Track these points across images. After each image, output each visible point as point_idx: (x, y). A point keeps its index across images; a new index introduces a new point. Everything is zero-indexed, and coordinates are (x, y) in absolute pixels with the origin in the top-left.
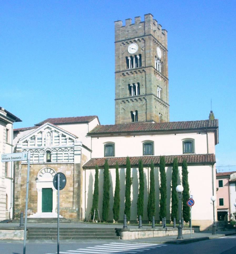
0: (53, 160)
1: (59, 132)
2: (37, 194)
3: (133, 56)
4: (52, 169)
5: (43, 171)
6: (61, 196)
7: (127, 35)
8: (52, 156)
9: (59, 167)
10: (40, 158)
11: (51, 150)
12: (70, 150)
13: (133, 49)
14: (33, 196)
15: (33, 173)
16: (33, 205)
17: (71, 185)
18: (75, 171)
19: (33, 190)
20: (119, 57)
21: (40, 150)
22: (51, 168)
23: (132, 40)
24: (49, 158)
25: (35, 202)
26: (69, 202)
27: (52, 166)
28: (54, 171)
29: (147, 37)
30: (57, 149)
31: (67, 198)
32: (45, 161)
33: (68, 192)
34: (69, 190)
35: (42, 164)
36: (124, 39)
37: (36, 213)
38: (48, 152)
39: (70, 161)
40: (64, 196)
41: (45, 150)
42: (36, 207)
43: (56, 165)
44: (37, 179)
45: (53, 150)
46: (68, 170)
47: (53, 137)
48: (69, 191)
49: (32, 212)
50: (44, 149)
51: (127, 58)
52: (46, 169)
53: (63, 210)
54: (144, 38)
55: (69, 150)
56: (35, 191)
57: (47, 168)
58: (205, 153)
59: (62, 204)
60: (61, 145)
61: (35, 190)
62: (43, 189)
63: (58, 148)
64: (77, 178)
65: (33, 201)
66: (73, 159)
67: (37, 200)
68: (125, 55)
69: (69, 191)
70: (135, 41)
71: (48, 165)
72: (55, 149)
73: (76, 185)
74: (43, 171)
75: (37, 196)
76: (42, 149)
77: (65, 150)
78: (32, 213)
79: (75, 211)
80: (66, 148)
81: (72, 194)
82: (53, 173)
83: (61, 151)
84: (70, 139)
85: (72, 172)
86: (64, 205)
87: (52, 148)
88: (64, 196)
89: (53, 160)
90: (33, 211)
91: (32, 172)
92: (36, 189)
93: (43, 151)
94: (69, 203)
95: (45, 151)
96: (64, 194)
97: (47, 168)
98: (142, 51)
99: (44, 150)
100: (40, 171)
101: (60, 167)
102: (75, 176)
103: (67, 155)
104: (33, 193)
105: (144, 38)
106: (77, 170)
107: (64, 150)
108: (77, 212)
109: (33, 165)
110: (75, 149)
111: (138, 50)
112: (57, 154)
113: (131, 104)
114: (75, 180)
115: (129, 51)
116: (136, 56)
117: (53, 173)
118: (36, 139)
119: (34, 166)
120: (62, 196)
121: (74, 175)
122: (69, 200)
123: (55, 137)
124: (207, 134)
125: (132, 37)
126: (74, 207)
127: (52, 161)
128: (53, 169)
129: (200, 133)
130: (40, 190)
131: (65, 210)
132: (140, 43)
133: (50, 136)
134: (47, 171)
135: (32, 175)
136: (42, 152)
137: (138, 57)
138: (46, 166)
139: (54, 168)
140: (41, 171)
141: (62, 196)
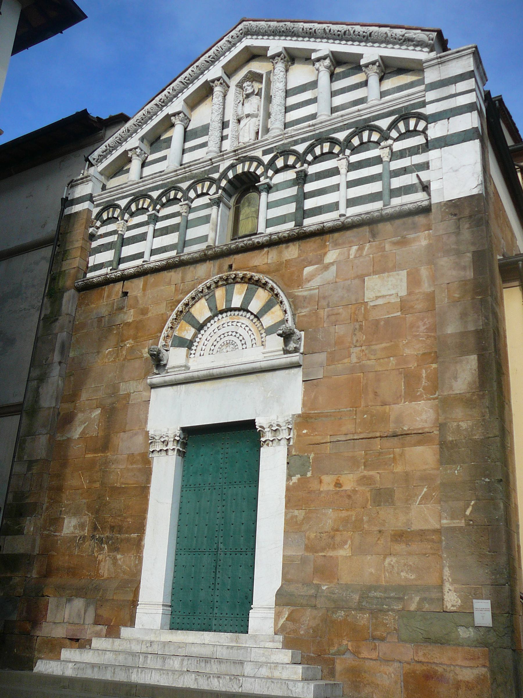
2: (147, 472)
4: (258, 283)
6: (328, 482)
9: (310, 264)
11: (260, 163)
12: (394, 134)
14: (116, 491)
16: (115, 559)
19: (126, 444)
21: (192, 186)
22: (249, 274)
25: (128, 540)
26: (400, 536)
27: (259, 259)
28: (278, 290)
30: (301, 148)
31: (382, 497)
33: (388, 443)
34: (392, 427)
37: (125, 632)
40: (349, 481)
41: (224, 175)
42: (132, 584)
44: (158, 362)
46: (382, 267)
48: (395, 436)
49: (96, 623)
50: (216, 169)
53: (341, 614)
55: (385, 137)
59: (331, 553)
61: (136, 444)
62: (192, 436)
63: (304, 140)
64: (463, 315)
65: (112, 528)
66: (426, 188)
67: (141, 529)
69: (395, 436)
75: (144, 491)
77: (356, 141)
79: (464, 633)
81: (423, 457)
82: (267, 308)
83: (330, 155)
86: (359, 567)
87: (265, 153)
90: (105, 612)
91: (128, 324)
92: (140, 439)
93: (213, 181)
94: (400, 547)
95: (224, 183)
96: (354, 463)
99: (216, 176)
100: (180, 307)
101: (320, 260)
103: (377, 169)
104: (121, 472)
106: (459, 253)
108: (483, 643)
109: (139, 282)
117: (267, 308)
119: (144, 289)
120: (338, 484)
122: (393, 519)
126: (447, 586)
128: (264, 279)
130: (171, 446)
131: (363, 619)
134: (229, 300)
135: (129, 344)
136: (203, 194)
138: (220, 271)
139: (273, 270)
140: (187, 305)
141: (338, 484)
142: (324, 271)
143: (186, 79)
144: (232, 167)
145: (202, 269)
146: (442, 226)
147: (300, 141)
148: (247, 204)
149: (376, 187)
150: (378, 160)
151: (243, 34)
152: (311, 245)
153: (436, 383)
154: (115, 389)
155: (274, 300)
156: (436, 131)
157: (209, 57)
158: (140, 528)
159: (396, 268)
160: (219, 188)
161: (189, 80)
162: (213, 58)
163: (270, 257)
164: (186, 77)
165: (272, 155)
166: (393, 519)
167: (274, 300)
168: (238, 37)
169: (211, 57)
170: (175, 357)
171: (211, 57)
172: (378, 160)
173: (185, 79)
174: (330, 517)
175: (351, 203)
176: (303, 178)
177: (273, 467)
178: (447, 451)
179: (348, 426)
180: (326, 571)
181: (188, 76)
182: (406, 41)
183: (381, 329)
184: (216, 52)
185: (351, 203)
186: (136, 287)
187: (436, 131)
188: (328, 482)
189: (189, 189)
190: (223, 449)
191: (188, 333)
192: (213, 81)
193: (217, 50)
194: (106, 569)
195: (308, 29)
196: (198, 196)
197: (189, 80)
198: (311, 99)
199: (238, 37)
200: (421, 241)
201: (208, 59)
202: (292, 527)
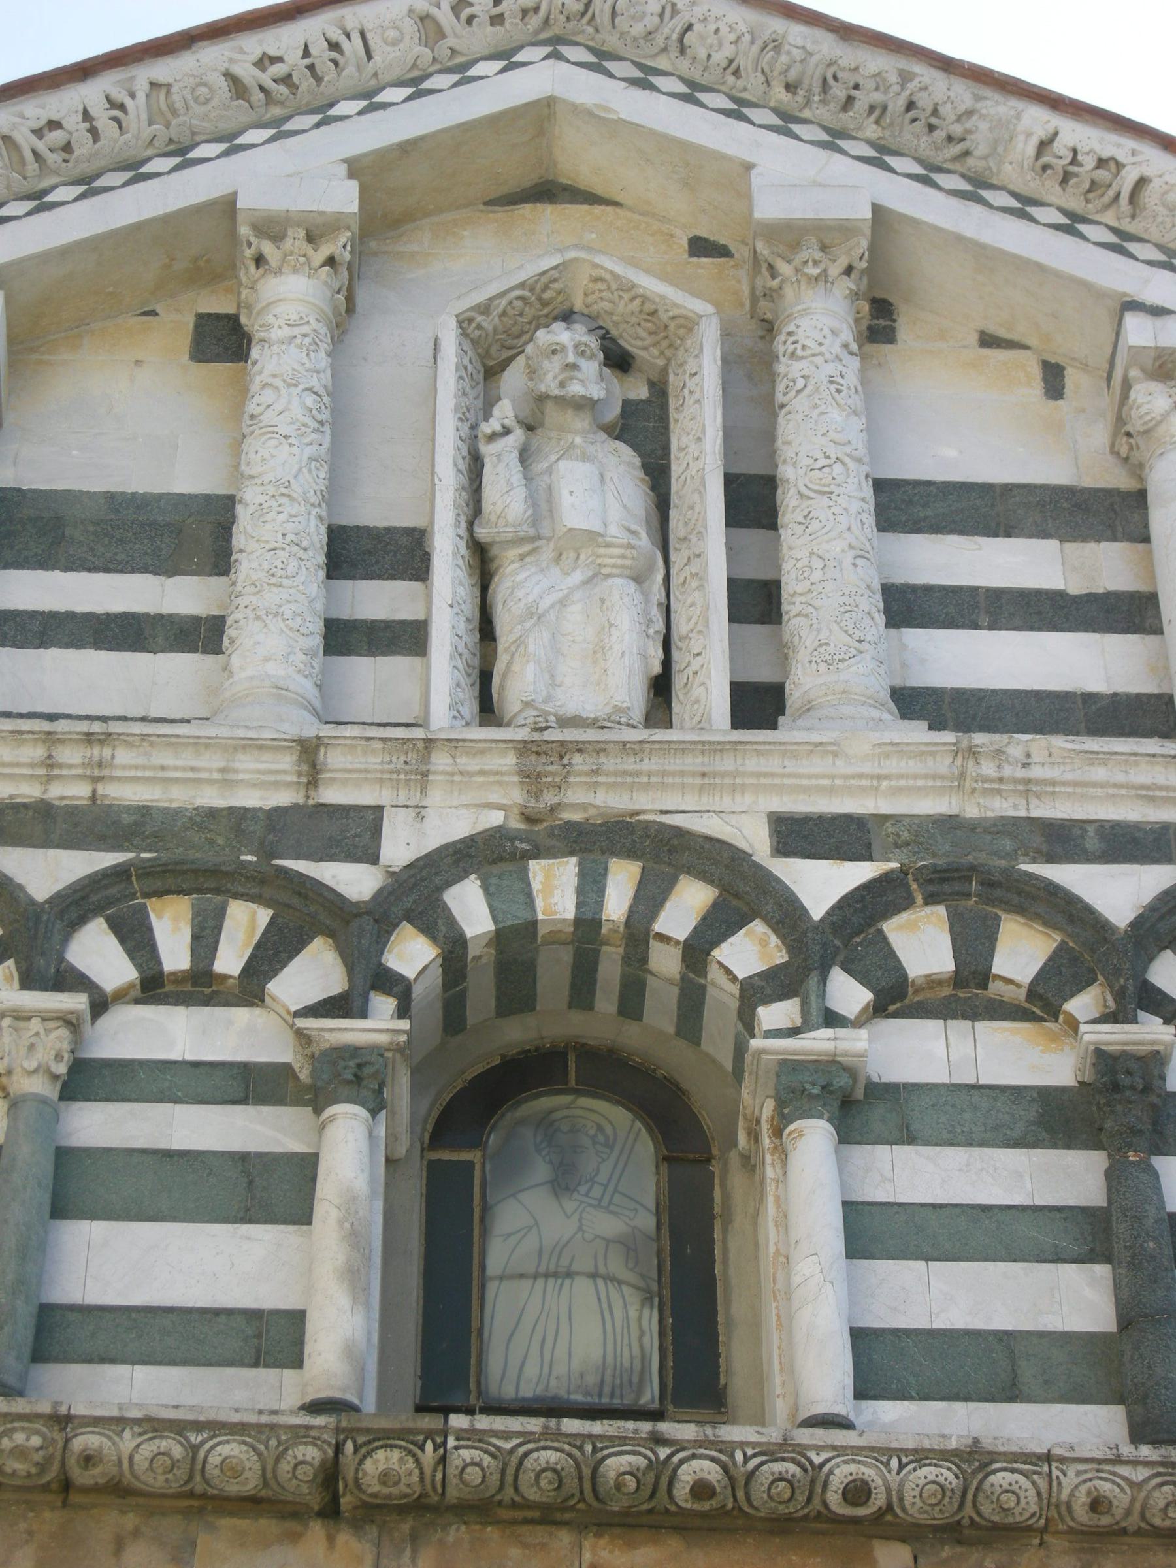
8: (809, 1178)
11: (746, 893)
21: (112, 901)
41: (416, 895)
45: (855, 930)
87: (800, 835)
89: (884, 1361)
93: (305, 915)
95: (411, 954)
99: (355, 881)
123: (903, 505)
133: (621, 464)
136: (200, 987)
143: (57, 137)
144: (491, 856)
147: (1092, 843)
148: (541, 1170)
151: (535, 21)
157: (265, 61)
160: (371, 979)
161: (67, 148)
162: (286, 80)
164: (54, 125)
165: (859, 873)
168: (497, 20)
169: (278, 70)
171: (278, 70)
173: (38, 133)
181: (74, 123)
184: (319, 49)
189: (77, 904)
192: (272, 228)
193: (334, 46)
195: (1089, 162)
196: (154, 987)
197: (67, 148)
198: (1061, 594)
199: (497, 20)
201: (246, 71)
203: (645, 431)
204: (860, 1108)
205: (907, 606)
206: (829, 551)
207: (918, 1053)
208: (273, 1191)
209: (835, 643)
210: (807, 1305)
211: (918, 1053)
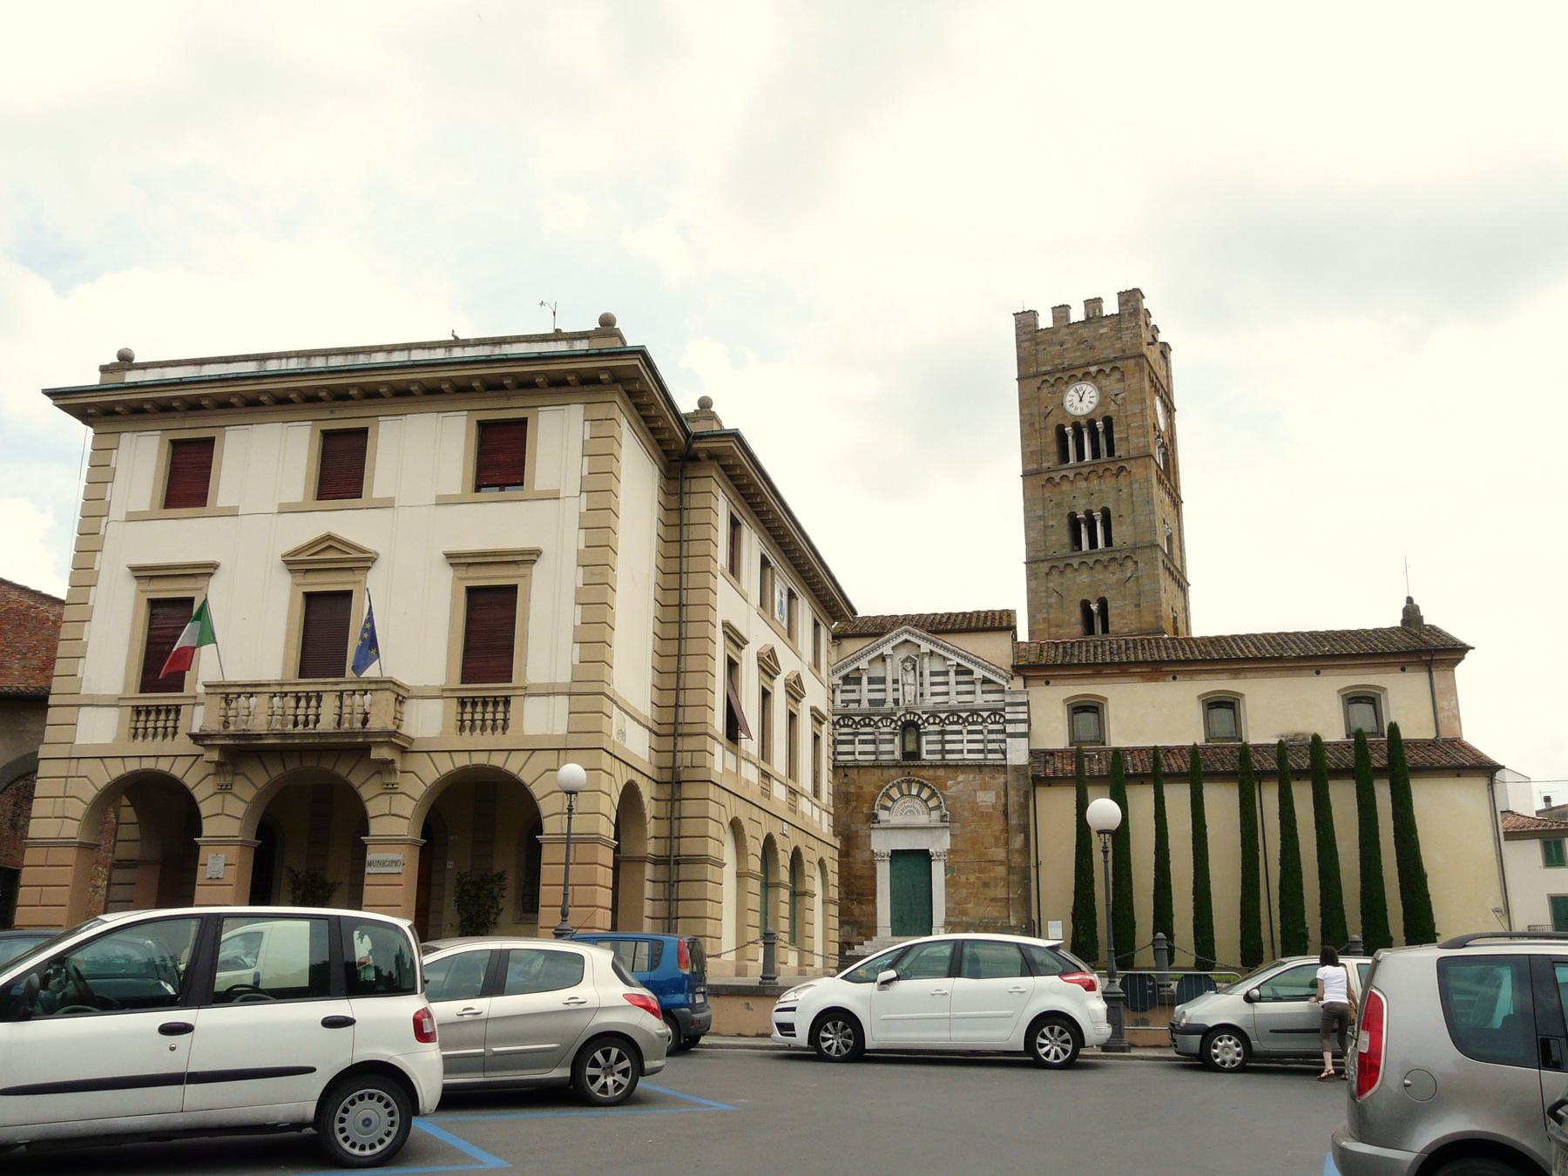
0: (928, 752)
1: (945, 658)
3: (1083, 422)
5: (895, 793)
6: (963, 878)
7: (1060, 355)
8: (924, 739)
10: (883, 747)
13: (1081, 400)
15: (859, 796)
17: (997, 839)
18: (1012, 793)
19: (860, 856)
20: (1032, 425)
23: (1079, 374)
24: (911, 747)
26: (993, 900)
27: (924, 773)
29: (1132, 362)
30: (943, 716)
31: (986, 885)
32: (898, 755)
35: (888, 767)
36: (1048, 368)
38: (910, 728)
39: (990, 756)
40: (972, 878)
43: (941, 772)
44: (873, 818)
46: (985, 788)
47: (926, 673)
49: (859, 934)
51: (1060, 430)
52: (904, 786)
54: (1118, 364)
55: (984, 721)
56: (864, 862)
57: (909, 782)
58: (1431, 735)
60: (954, 700)
61: (867, 855)
62: (896, 855)
66: (1004, 752)
68: (1053, 421)
70: (1087, 374)
71: (913, 771)
72: (935, 716)
73: (1018, 842)
74: (895, 793)
75: (873, 878)
76: (886, 716)
78: (855, 939)
80: (974, 712)
81: (1001, 871)
82: (930, 798)
83: (957, 723)
84: (985, 681)
85: (998, 797)
88: (972, 878)
89: (928, 752)
97: (909, 782)
98: (1113, 407)
102: (1010, 809)
103: (979, 737)
104: (859, 869)
105: (1118, 364)
107: (966, 720)
110: (1008, 717)
111: (1100, 404)
112: (942, 733)
113: (1084, 577)
114: (1014, 821)
115: (1067, 405)
116: (1091, 424)
117: (930, 798)
118: (865, 680)
121: (1006, 805)
122: (991, 893)
123: (933, 674)
124: (1430, 672)
125: (1077, 363)
127: (924, 756)
129: (1403, 670)
132: (1104, 382)
137: (1099, 424)
139: (934, 779)
142: (958, 785)
145: (893, 772)
146: (1011, 777)
149: (980, 746)
150: (981, 732)
152: (951, 773)
153: (1007, 843)
154: (849, 827)
155: (933, 795)
156: (1010, 728)
158: (874, 894)
159: (990, 789)
163: (931, 772)
166: (991, 893)
167: (933, 795)
170: (883, 815)
172: (981, 732)
174: (964, 892)
175: (969, 751)
176: (942, 733)
177: (938, 870)
178: (1010, 870)
179: (971, 856)
180: (964, 913)
182: (994, 672)
183: (984, 817)
185: (969, 751)
186: (853, 774)
187: (1010, 728)
188: (963, 878)
190: (913, 863)
191: (889, 804)
194: (857, 911)
200: (1001, 779)
202: (947, 895)
203: (914, 669)
204: (926, 734)
205: (932, 684)
206: (927, 679)
207: (931, 728)
208: (892, 741)
209: (928, 689)
210: (925, 747)
211: (931, 728)
